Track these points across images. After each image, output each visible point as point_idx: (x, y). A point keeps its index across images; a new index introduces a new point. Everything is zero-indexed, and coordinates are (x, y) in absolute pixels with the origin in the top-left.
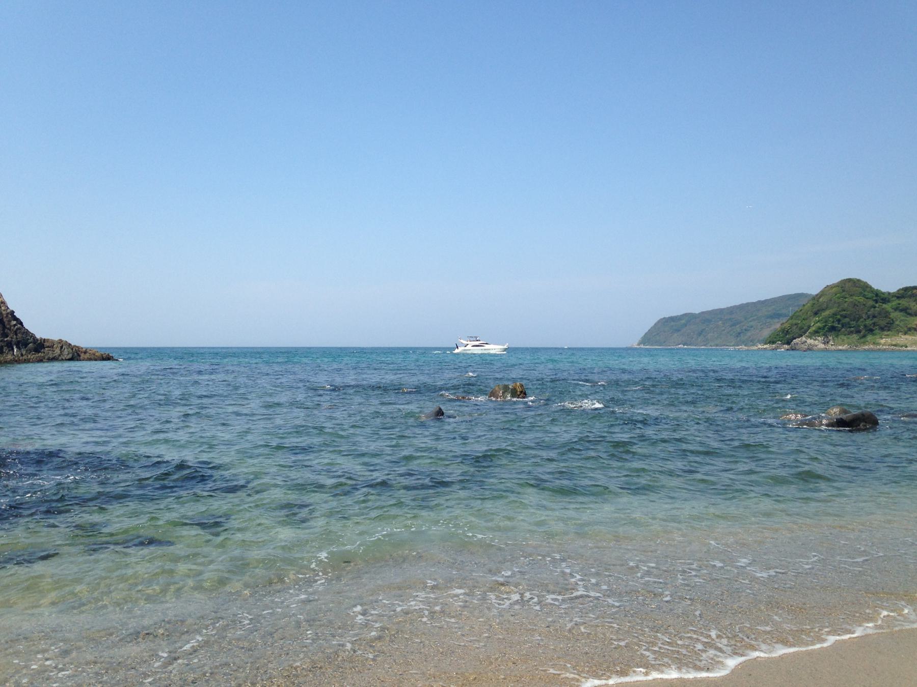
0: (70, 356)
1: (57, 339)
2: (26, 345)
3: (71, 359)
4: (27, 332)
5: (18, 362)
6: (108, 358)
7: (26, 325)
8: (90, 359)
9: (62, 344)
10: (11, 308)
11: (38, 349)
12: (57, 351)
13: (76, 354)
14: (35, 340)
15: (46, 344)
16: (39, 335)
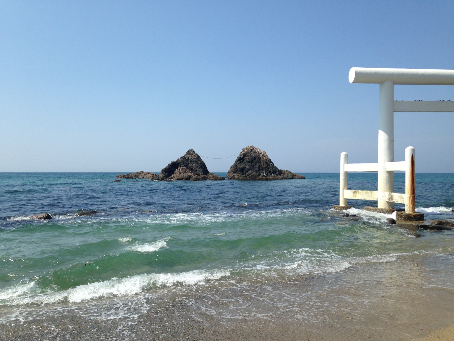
0: (291, 177)
1: (286, 170)
2: (276, 172)
3: (292, 178)
4: (276, 167)
5: (274, 179)
6: (304, 178)
7: (275, 165)
8: (298, 178)
9: (288, 172)
10: (269, 158)
11: (280, 174)
12: (287, 175)
13: (293, 177)
14: (279, 171)
15: (282, 172)
16: (280, 168)
